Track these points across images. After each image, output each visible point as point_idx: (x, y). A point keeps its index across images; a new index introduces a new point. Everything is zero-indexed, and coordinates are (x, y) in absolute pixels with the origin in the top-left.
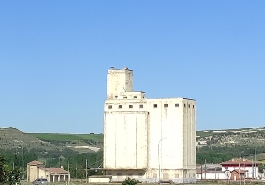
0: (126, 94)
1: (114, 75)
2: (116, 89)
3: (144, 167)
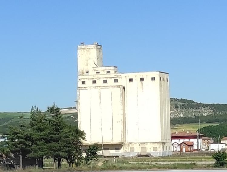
0: (98, 69)
1: (84, 50)
2: (87, 65)
3: (121, 141)
